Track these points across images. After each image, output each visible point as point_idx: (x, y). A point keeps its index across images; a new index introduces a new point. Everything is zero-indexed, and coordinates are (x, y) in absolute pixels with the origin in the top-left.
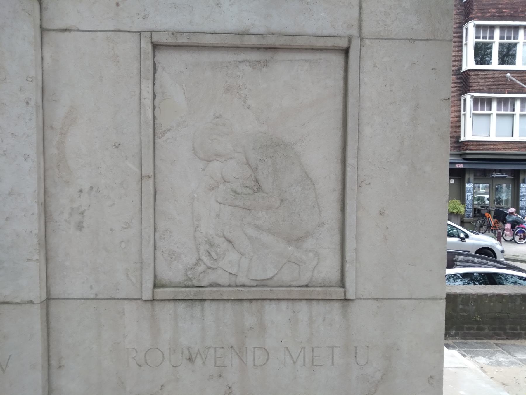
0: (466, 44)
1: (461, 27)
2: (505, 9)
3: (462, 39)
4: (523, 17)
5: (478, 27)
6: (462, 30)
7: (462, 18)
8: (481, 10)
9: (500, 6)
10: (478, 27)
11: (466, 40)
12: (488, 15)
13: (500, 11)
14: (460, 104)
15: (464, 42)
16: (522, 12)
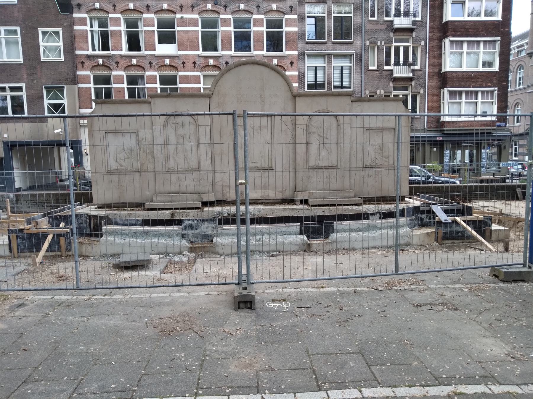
0: (444, 53)
1: (440, 41)
2: (470, 29)
3: (442, 49)
4: (483, 34)
5: (452, 42)
6: (442, 43)
7: (442, 34)
8: (454, 30)
9: (467, 27)
10: (452, 42)
11: (444, 51)
12: (459, 33)
13: (467, 30)
14: (441, 96)
15: (443, 52)
16: (482, 31)
